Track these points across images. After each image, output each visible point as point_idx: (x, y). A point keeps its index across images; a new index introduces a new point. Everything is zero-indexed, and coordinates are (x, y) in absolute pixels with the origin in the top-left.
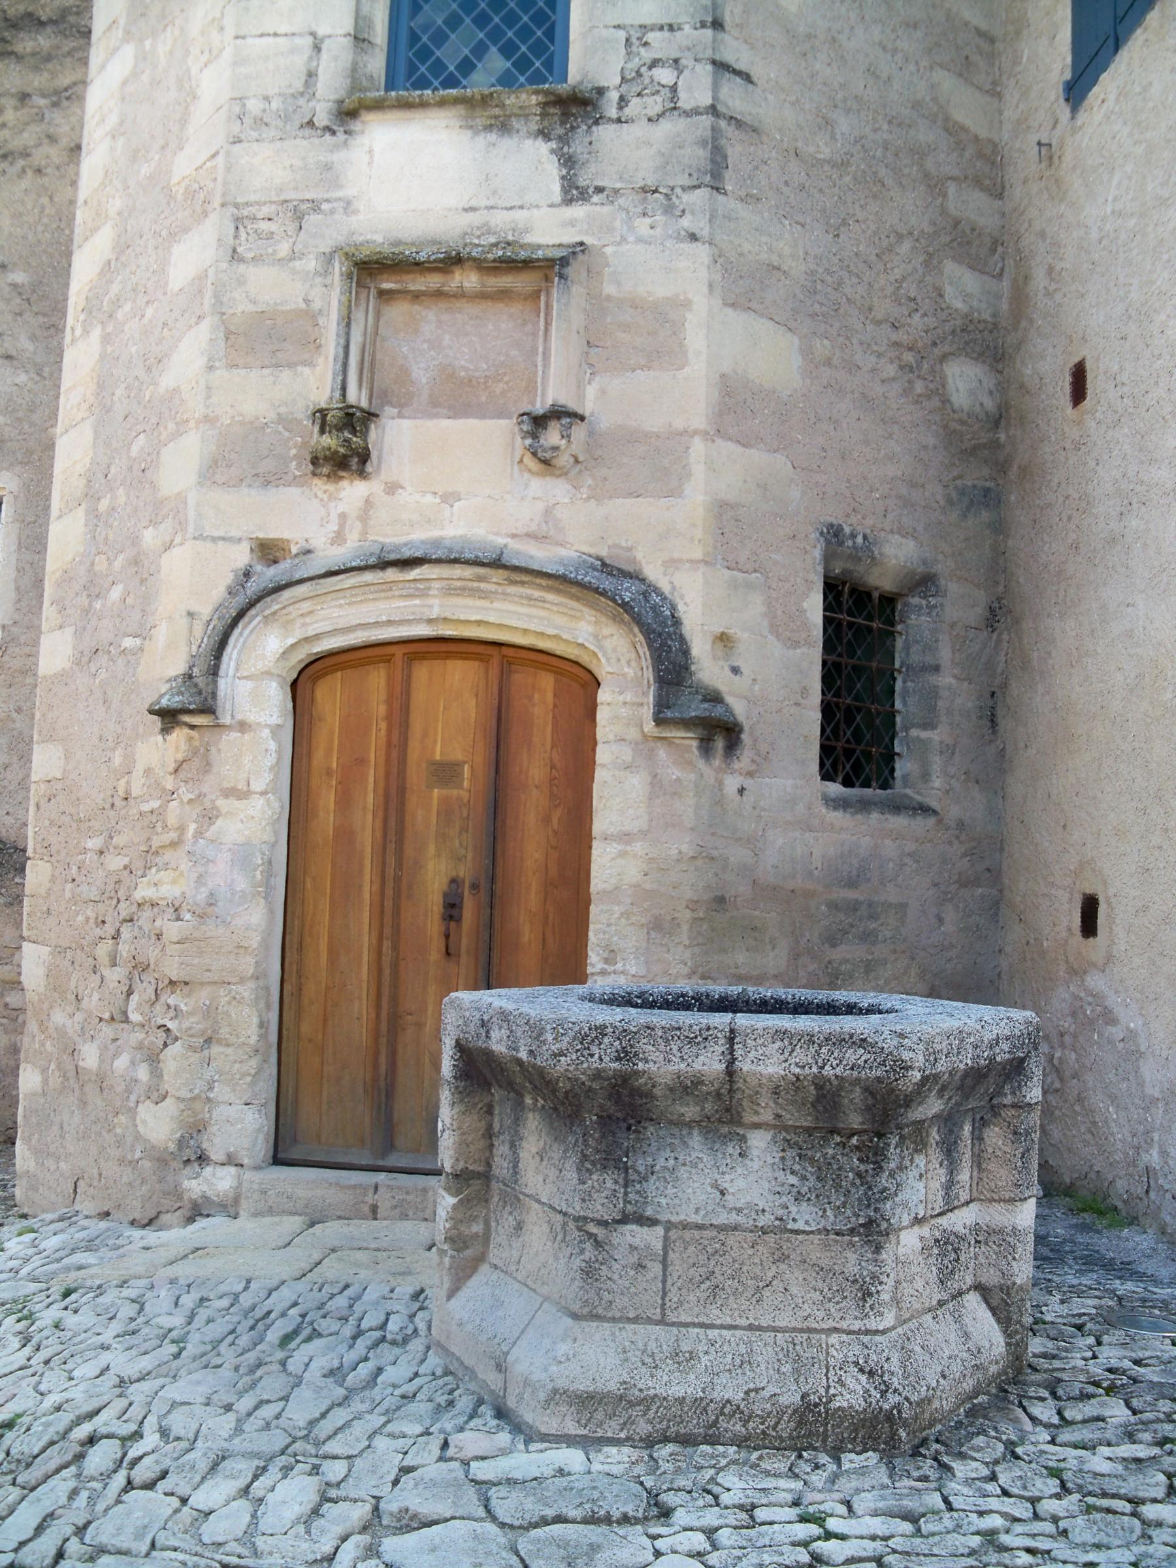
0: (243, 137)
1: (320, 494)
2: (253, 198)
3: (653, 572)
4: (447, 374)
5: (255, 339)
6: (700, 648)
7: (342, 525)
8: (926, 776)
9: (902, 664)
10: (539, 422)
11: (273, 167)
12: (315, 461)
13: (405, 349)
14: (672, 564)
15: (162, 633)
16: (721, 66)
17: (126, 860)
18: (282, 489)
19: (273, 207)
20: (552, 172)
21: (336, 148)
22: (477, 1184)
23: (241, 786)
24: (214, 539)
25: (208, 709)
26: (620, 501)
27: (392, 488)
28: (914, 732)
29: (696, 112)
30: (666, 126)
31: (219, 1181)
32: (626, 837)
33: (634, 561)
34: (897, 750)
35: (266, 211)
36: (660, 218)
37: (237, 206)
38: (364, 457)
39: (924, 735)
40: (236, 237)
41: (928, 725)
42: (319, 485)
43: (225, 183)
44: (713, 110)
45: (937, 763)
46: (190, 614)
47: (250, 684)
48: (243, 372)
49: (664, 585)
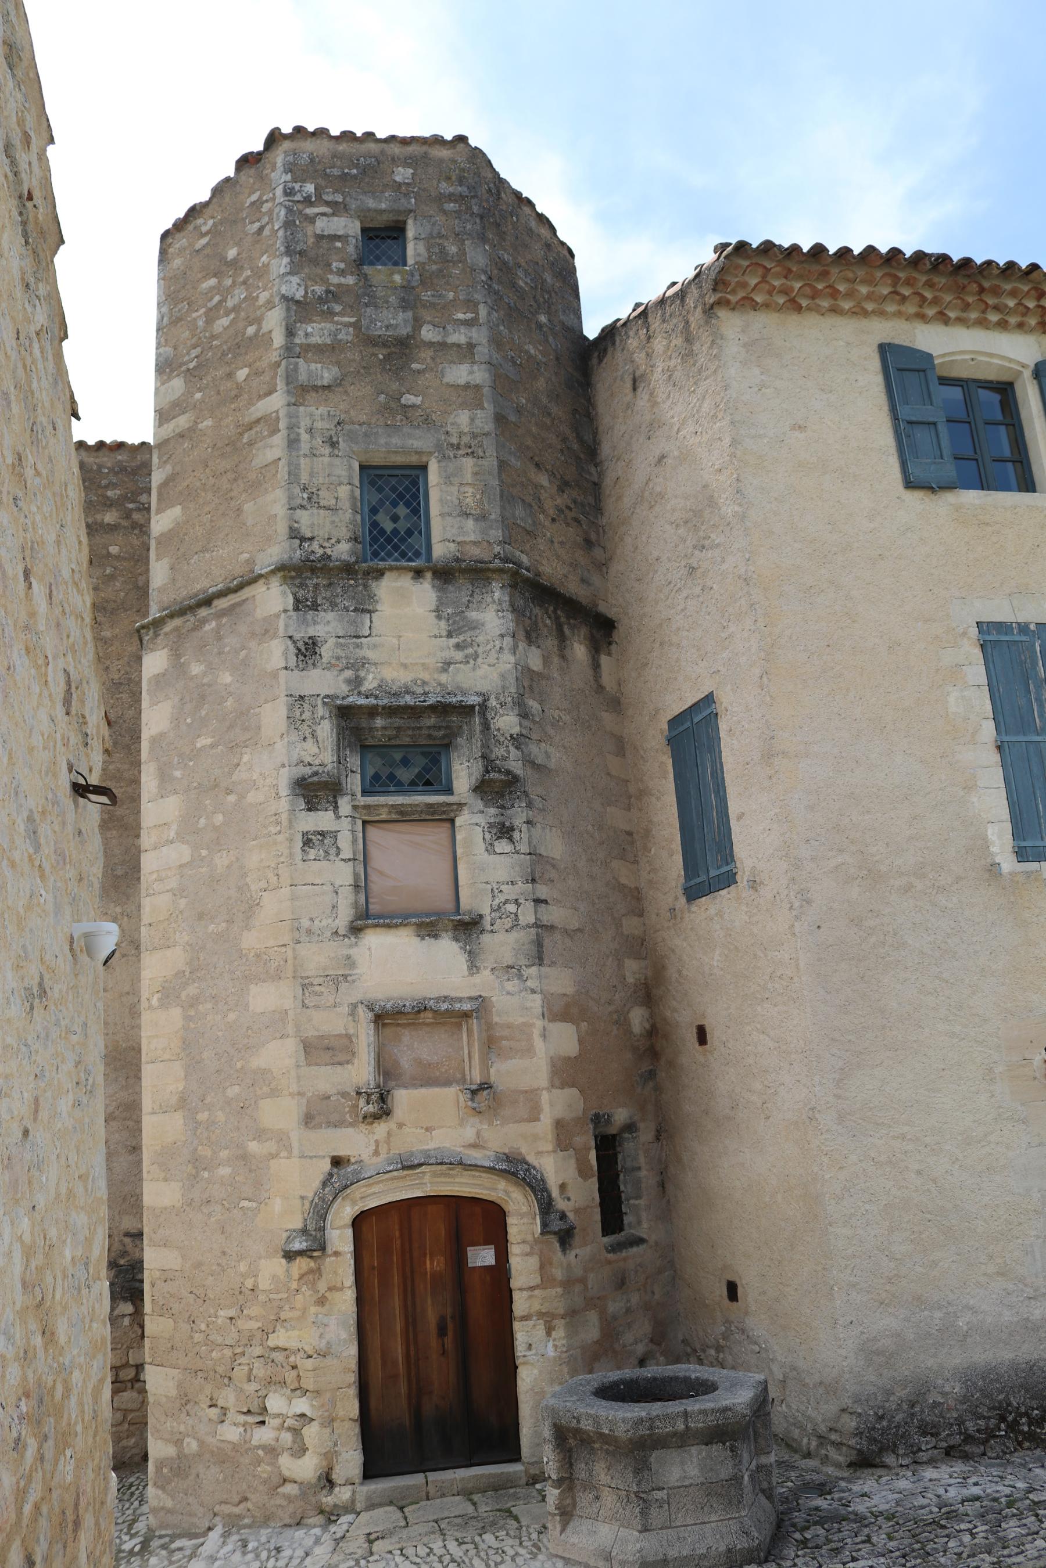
0: (301, 940)
2: (310, 974)
3: (531, 1159)
5: (322, 1050)
6: (555, 1193)
7: (377, 1146)
8: (639, 1223)
9: (623, 1167)
11: (318, 957)
14: (539, 1153)
15: (277, 1205)
16: (538, 901)
17: (260, 1324)
19: (322, 979)
20: (461, 960)
21: (351, 946)
22: (567, 1482)
23: (339, 1285)
24: (311, 1157)
25: (323, 1248)
27: (400, 1125)
28: (632, 1202)
29: (528, 926)
30: (514, 935)
31: (343, 1494)
32: (532, 1288)
33: (520, 1154)
34: (624, 1210)
35: (316, 981)
36: (516, 981)
37: (302, 978)
39: (637, 1202)
40: (304, 994)
41: (638, 1197)
42: (363, 1127)
43: (294, 966)
44: (536, 925)
45: (644, 1215)
46: (302, 1198)
47: (338, 1232)
48: (316, 1068)
49: (535, 1163)
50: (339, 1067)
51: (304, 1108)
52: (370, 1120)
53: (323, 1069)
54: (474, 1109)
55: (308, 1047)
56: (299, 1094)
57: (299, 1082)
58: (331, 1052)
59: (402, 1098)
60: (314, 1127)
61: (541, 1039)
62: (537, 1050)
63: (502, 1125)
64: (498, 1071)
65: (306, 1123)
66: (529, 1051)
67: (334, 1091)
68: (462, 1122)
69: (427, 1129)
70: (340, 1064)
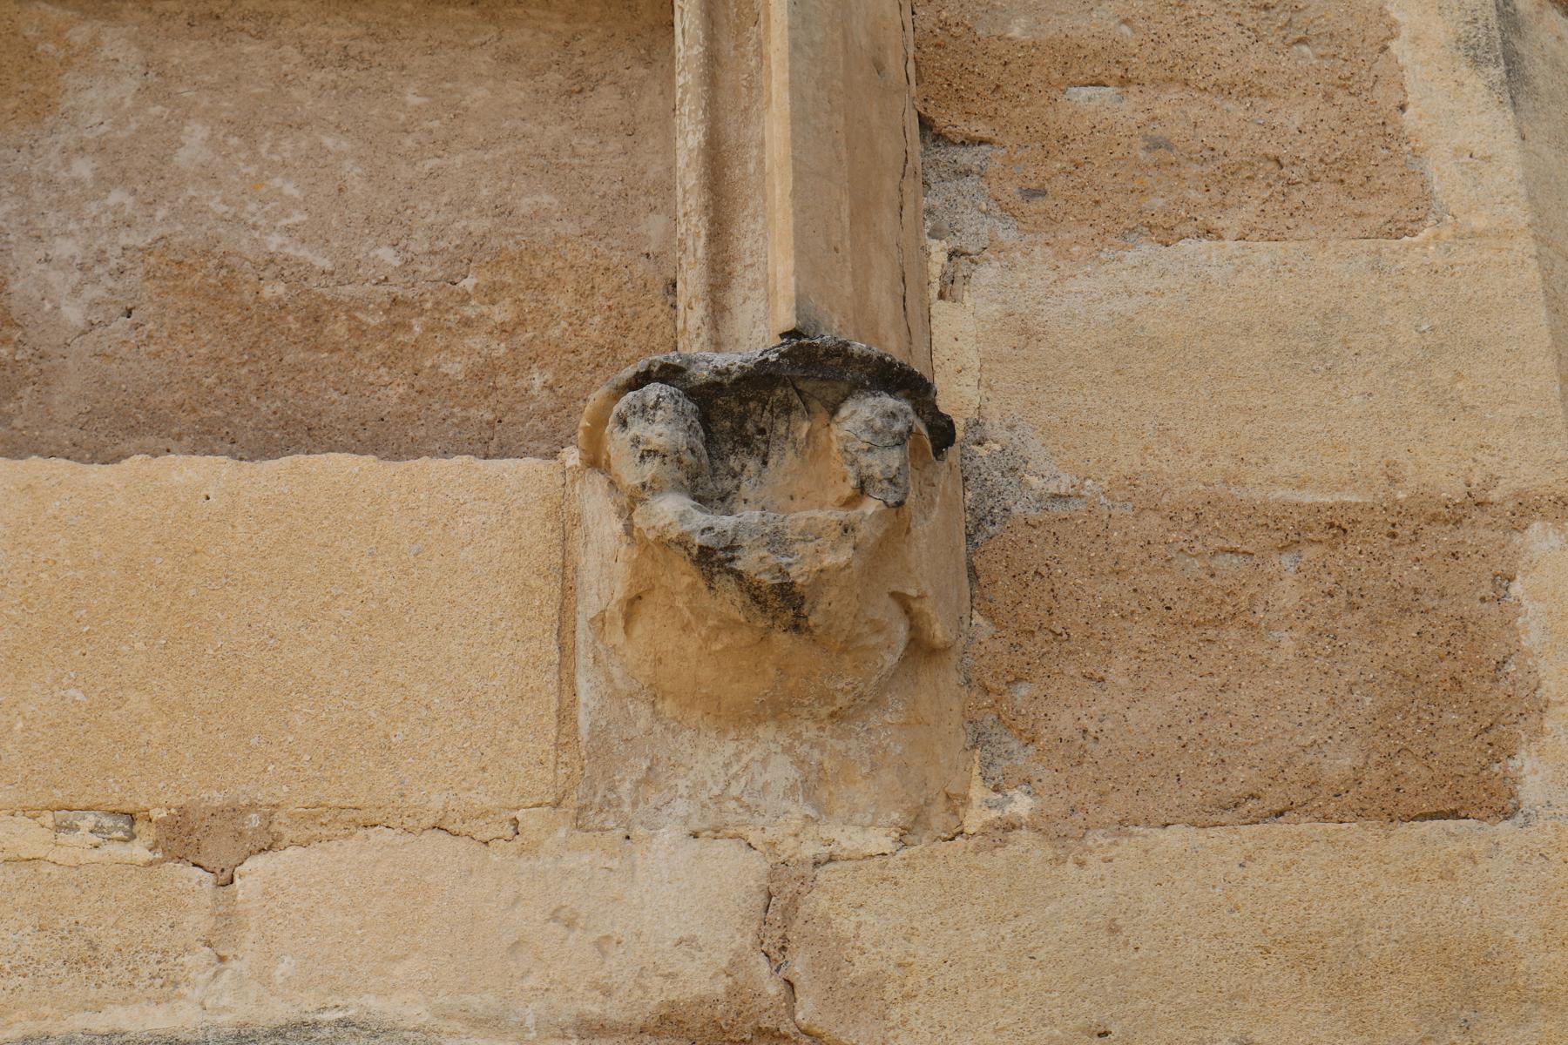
4: (205, 284)
10: (733, 415)
26: (1175, 838)
54: (712, 560)
61: (1479, 85)
62: (1443, 174)
63: (1061, 832)
64: (1028, 333)
66: (1359, 170)
68: (591, 788)
69: (182, 838)
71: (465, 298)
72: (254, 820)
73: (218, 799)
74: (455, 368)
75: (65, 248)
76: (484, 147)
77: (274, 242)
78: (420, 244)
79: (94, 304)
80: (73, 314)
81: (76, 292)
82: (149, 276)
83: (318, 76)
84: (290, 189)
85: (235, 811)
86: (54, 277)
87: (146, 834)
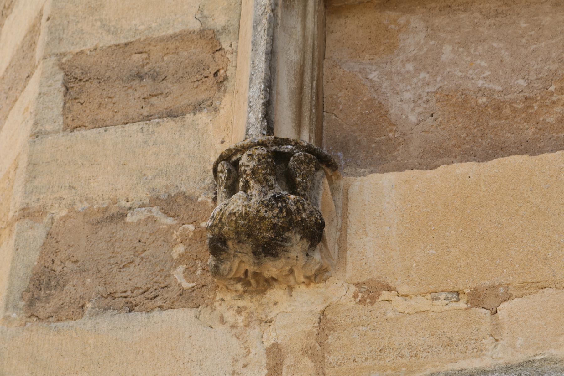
1: (230, 316)
4: (458, 102)
12: (218, 245)
13: (373, 76)
18: (157, 315)
27: (370, 291)
38: (315, 234)
42: (228, 304)
50: (169, 123)
51: (34, 257)
52: (241, 261)
53: (114, 134)
55: (76, 81)
56: (26, 213)
57: (31, 177)
58: (148, 85)
59: (377, 204)
60: (56, 316)
65: (31, 303)
67: (144, 195)
69: (477, 298)
70: (172, 114)
71: (552, 94)
72: (501, 290)
73: (488, 283)
74: (551, 119)
75: (407, 96)
76: (552, 38)
77: (480, 83)
78: (532, 77)
79: (420, 114)
80: (413, 118)
81: (413, 110)
82: (437, 101)
83: (488, 22)
84: (483, 64)
85: (494, 287)
86: (405, 106)
87: (464, 298)
